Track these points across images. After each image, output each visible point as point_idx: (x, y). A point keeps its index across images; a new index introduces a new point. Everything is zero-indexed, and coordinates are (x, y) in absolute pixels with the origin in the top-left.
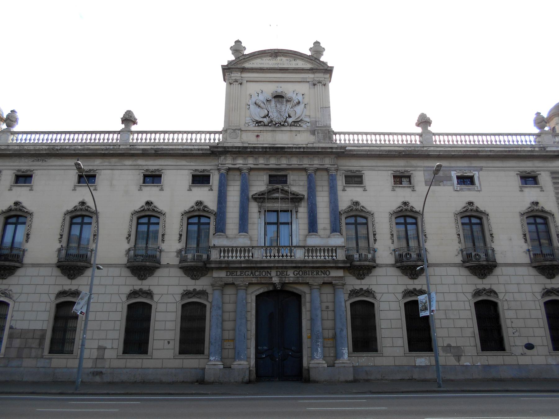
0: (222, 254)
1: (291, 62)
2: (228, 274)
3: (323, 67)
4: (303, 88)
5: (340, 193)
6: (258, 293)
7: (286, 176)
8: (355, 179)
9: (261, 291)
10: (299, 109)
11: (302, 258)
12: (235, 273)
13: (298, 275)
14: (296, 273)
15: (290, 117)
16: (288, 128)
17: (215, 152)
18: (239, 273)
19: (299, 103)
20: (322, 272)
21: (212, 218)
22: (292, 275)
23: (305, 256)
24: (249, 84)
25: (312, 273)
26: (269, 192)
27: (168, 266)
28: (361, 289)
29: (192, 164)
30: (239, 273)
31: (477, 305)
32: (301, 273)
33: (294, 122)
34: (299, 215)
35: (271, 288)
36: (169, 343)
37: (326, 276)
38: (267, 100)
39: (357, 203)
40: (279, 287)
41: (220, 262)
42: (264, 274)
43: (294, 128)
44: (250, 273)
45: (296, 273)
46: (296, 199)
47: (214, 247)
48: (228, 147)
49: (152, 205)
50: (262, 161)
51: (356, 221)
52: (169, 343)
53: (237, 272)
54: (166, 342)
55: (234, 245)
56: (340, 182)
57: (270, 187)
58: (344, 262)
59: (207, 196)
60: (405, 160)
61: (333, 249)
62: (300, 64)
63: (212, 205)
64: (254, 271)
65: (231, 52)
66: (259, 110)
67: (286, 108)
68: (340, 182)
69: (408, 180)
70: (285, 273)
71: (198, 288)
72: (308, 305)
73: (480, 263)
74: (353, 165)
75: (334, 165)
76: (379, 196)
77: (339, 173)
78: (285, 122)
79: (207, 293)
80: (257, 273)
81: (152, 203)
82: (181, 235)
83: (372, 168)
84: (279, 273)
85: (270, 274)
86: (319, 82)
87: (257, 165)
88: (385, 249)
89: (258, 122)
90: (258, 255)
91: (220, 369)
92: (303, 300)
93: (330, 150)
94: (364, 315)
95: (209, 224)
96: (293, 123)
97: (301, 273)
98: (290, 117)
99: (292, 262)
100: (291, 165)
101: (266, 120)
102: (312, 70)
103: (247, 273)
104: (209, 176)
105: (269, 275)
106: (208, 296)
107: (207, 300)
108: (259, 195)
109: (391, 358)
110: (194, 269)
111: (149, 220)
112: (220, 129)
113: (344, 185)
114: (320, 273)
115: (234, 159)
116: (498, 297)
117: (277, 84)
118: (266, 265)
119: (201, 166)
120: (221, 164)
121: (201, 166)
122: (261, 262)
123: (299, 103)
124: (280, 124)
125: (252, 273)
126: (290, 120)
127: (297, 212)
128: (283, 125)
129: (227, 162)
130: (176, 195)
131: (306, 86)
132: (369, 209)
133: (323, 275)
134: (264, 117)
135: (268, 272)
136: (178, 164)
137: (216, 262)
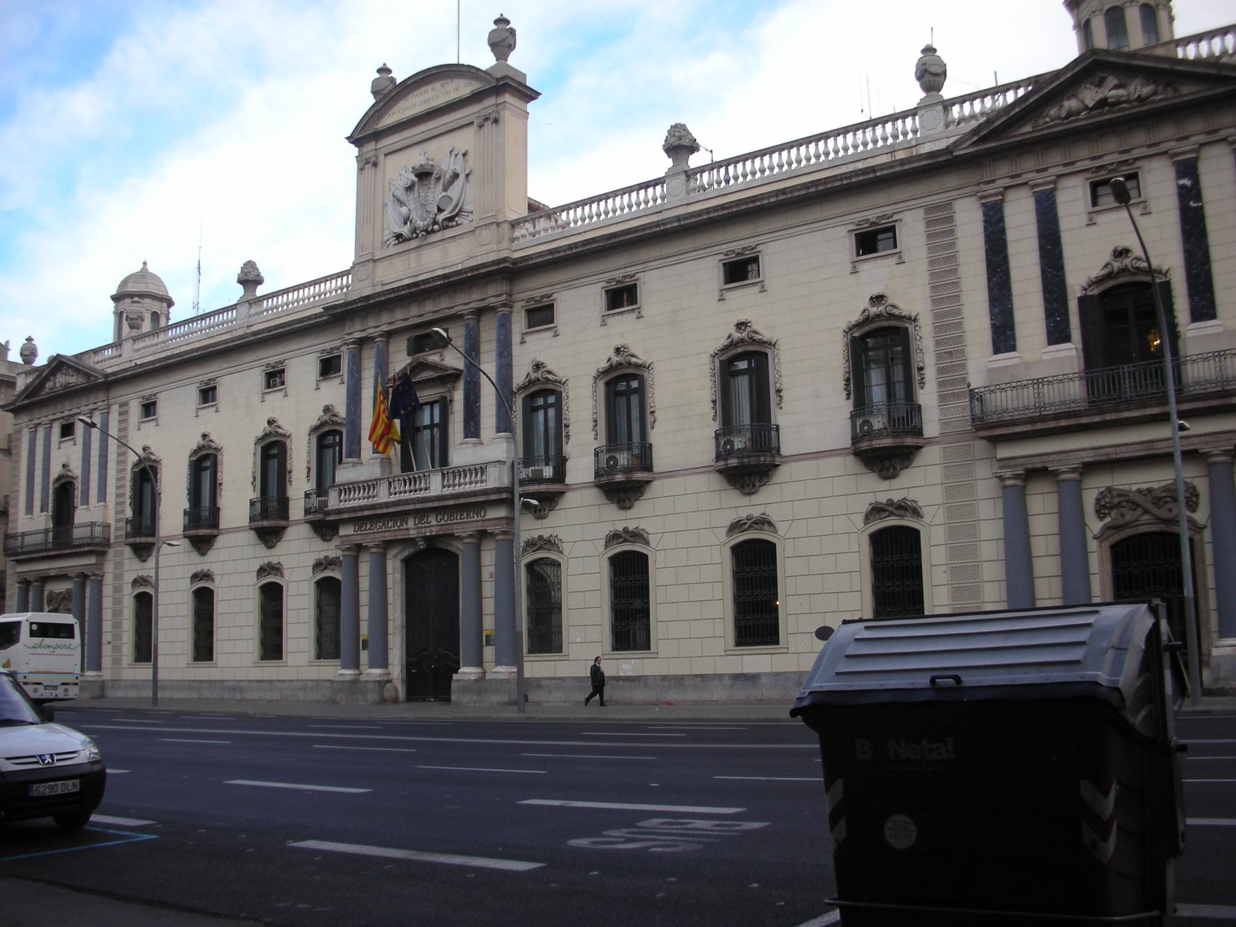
4: (465, 140)
5: (516, 349)
6: (403, 556)
9: (406, 553)
10: (454, 192)
15: (440, 210)
16: (438, 236)
17: (338, 316)
19: (456, 176)
22: (434, 522)
23: (444, 487)
24: (389, 158)
27: (297, 522)
28: (541, 537)
29: (319, 341)
31: (737, 550)
33: (451, 219)
43: (448, 233)
46: (449, 377)
55: (362, 478)
56: (519, 323)
59: (335, 394)
60: (725, 223)
62: (463, 88)
63: (341, 410)
67: (435, 194)
68: (519, 323)
73: (749, 459)
74: (531, 289)
75: (501, 295)
76: (575, 345)
77: (515, 309)
78: (435, 223)
82: (309, 469)
83: (569, 284)
86: (487, 119)
89: (399, 237)
90: (383, 495)
99: (425, 500)
101: (405, 230)
102: (476, 97)
110: (324, 527)
112: (347, 265)
116: (776, 532)
117: (417, 150)
118: (385, 511)
119: (328, 342)
123: (456, 176)
126: (441, 217)
128: (433, 232)
130: (305, 402)
131: (470, 132)
136: (303, 345)
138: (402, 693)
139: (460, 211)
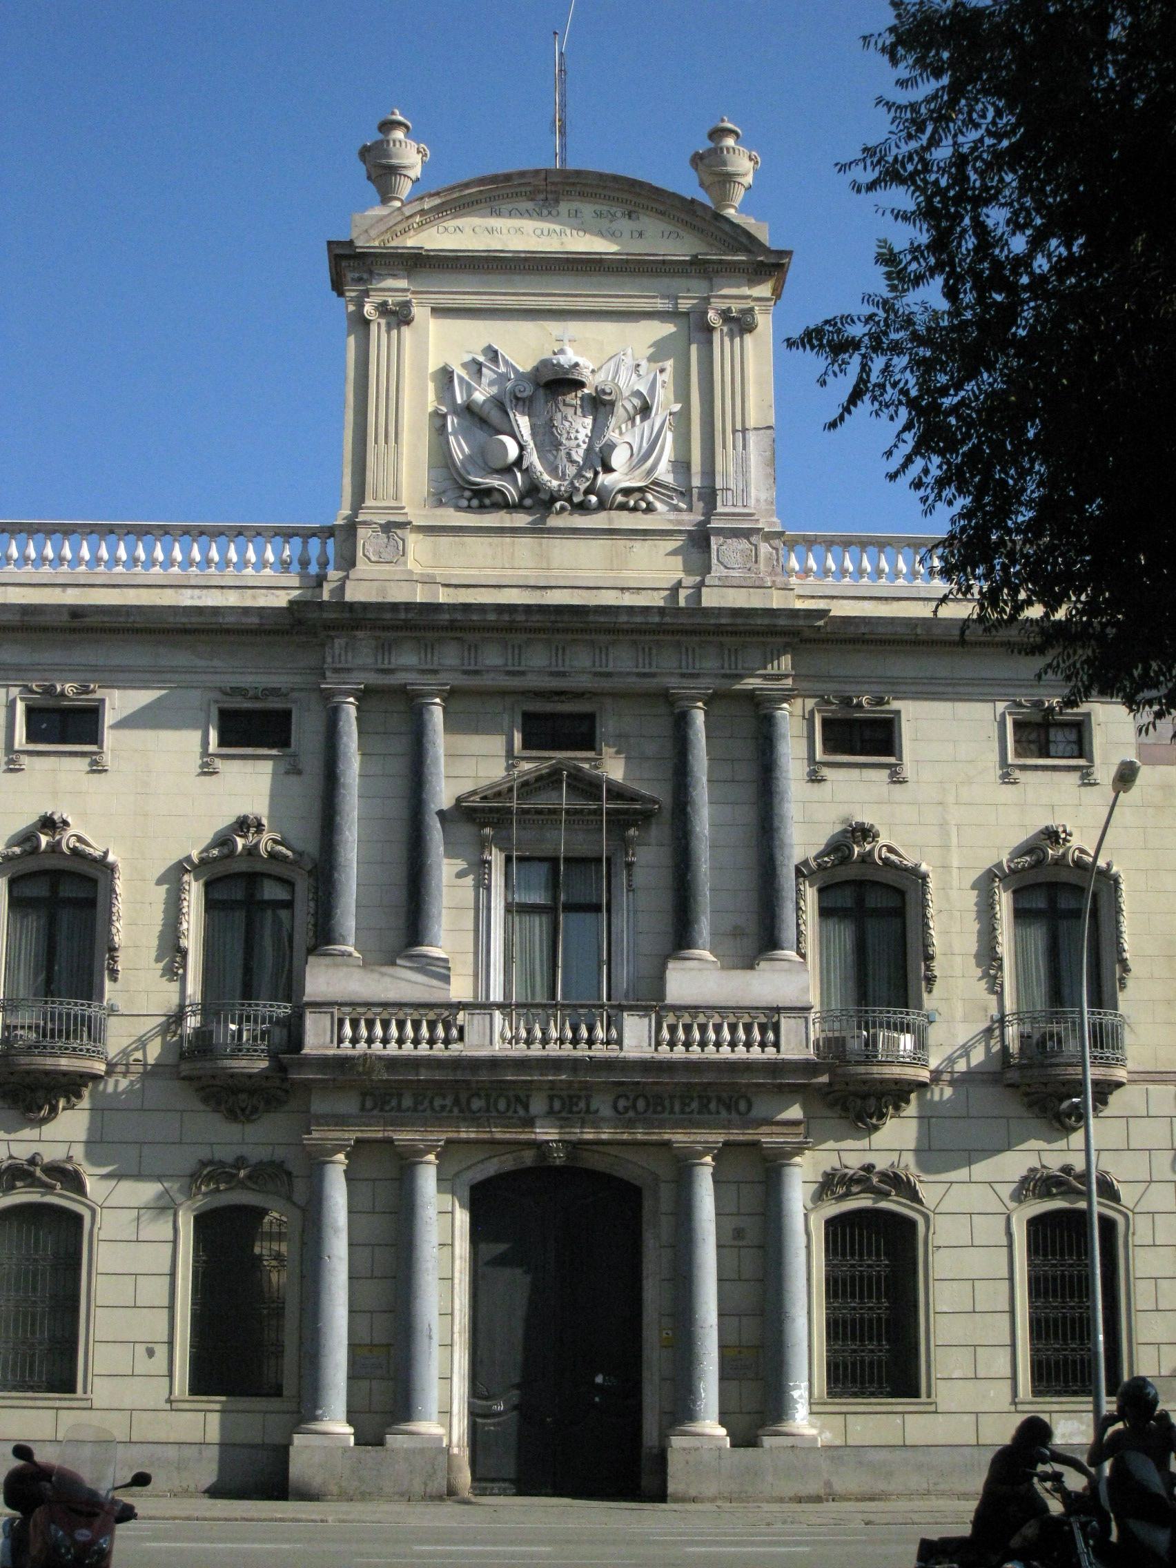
0: (348, 1031)
1: (615, 226)
2: (369, 1104)
3: (748, 251)
7: (590, 718)
8: (864, 737)
9: (491, 1168)
11: (647, 1053)
12: (394, 1103)
13: (631, 1114)
14: (622, 1103)
18: (407, 1102)
20: (719, 1099)
21: (303, 887)
23: (658, 1044)
25: (684, 1105)
26: (528, 787)
30: (407, 1102)
32: (641, 1104)
34: (640, 876)
35: (528, 1158)
36: (151, 1353)
37: (734, 1116)
38: (517, 399)
39: (864, 833)
40: (559, 1157)
41: (342, 1063)
42: (502, 1105)
44: (448, 1102)
45: (622, 1103)
47: (317, 1005)
48: (365, 606)
49: (71, 831)
50: (492, 657)
51: (860, 901)
52: (151, 1353)
53: (400, 1096)
54: (140, 1349)
57: (526, 766)
58: (807, 1067)
61: (769, 1019)
64: (463, 1097)
65: (362, 169)
66: (481, 435)
69: (1073, 736)
70: (582, 1105)
71: (257, 1154)
72: (666, 1223)
79: (289, 1174)
80: (477, 1104)
81: (65, 823)
84: (557, 1105)
85: (526, 1107)
87: (476, 672)
88: (962, 1010)
91: (346, 1449)
92: (647, 1204)
93: (766, 621)
94: (879, 1257)
95: (289, 905)
96: (620, 498)
97: (641, 1104)
98: (608, 469)
100: (609, 675)
103: (438, 1102)
104: (287, 714)
105: (521, 1112)
106: (290, 1184)
107: (289, 1199)
108: (484, 798)
109: (966, 1418)
111: (54, 888)
113: (819, 755)
114: (713, 1106)
115: (385, 648)
120: (336, 671)
121: (258, 675)
122: (494, 1063)
124: (569, 499)
125: (457, 1102)
127: (629, 865)
129: (359, 661)
132: (910, 858)
133: (724, 1114)
134: (506, 471)
135: (518, 1099)
137: (324, 1063)
138: (465, 1477)
139: (654, 483)
